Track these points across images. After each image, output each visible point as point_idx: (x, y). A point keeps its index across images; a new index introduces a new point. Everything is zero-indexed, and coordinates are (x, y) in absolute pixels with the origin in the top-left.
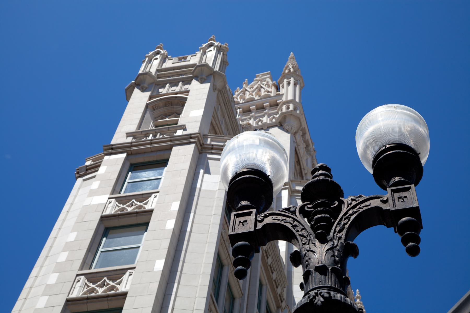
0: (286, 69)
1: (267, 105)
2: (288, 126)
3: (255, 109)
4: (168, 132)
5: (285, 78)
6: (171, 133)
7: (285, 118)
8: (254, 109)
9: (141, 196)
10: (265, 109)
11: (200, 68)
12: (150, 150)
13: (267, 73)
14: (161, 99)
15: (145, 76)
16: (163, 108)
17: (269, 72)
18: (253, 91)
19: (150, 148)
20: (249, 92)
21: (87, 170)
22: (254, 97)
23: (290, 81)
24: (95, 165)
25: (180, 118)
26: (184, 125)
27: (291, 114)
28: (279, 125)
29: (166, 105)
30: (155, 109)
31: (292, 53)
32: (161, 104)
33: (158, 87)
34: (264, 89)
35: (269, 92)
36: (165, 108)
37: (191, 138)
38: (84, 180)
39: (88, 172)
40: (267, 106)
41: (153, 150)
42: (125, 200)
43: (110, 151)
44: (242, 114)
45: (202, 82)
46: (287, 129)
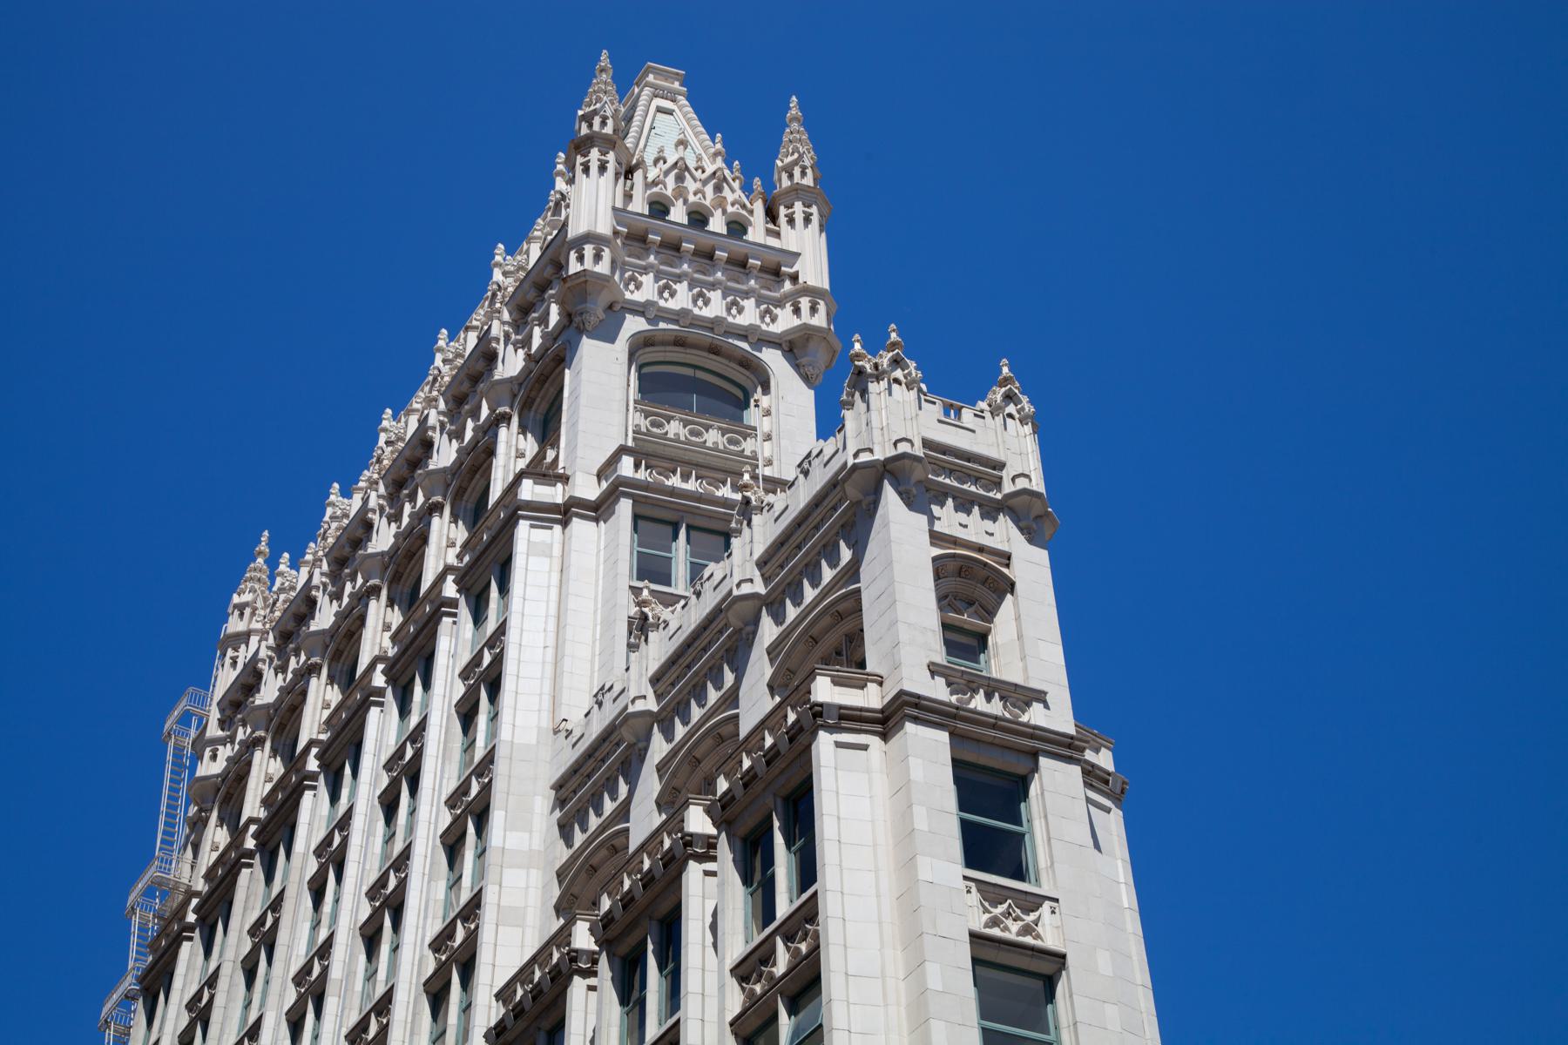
0: (797, 164)
1: (757, 265)
2: (813, 368)
3: (725, 259)
4: (1013, 695)
5: (798, 199)
6: (1018, 699)
7: (808, 340)
8: (721, 260)
9: (1023, 897)
10: (747, 271)
11: (1030, 498)
12: (991, 740)
13: (677, 74)
14: (954, 556)
15: (915, 464)
16: (954, 579)
17: (684, 72)
18: (705, 182)
19: (995, 737)
20: (695, 180)
21: (841, 718)
22: (707, 203)
23: (811, 214)
24: (859, 713)
25: (992, 625)
26: (1045, 693)
27: (825, 338)
28: (786, 349)
29: (960, 572)
30: (941, 575)
31: (794, 98)
32: (952, 566)
33: (928, 495)
34: (733, 191)
35: (744, 206)
36: (958, 579)
37: (1069, 746)
38: (839, 745)
39: (845, 724)
40: (754, 267)
41: (996, 741)
42: (994, 893)
43: (915, 712)
44: (690, 257)
45: (1031, 541)
46: (808, 373)
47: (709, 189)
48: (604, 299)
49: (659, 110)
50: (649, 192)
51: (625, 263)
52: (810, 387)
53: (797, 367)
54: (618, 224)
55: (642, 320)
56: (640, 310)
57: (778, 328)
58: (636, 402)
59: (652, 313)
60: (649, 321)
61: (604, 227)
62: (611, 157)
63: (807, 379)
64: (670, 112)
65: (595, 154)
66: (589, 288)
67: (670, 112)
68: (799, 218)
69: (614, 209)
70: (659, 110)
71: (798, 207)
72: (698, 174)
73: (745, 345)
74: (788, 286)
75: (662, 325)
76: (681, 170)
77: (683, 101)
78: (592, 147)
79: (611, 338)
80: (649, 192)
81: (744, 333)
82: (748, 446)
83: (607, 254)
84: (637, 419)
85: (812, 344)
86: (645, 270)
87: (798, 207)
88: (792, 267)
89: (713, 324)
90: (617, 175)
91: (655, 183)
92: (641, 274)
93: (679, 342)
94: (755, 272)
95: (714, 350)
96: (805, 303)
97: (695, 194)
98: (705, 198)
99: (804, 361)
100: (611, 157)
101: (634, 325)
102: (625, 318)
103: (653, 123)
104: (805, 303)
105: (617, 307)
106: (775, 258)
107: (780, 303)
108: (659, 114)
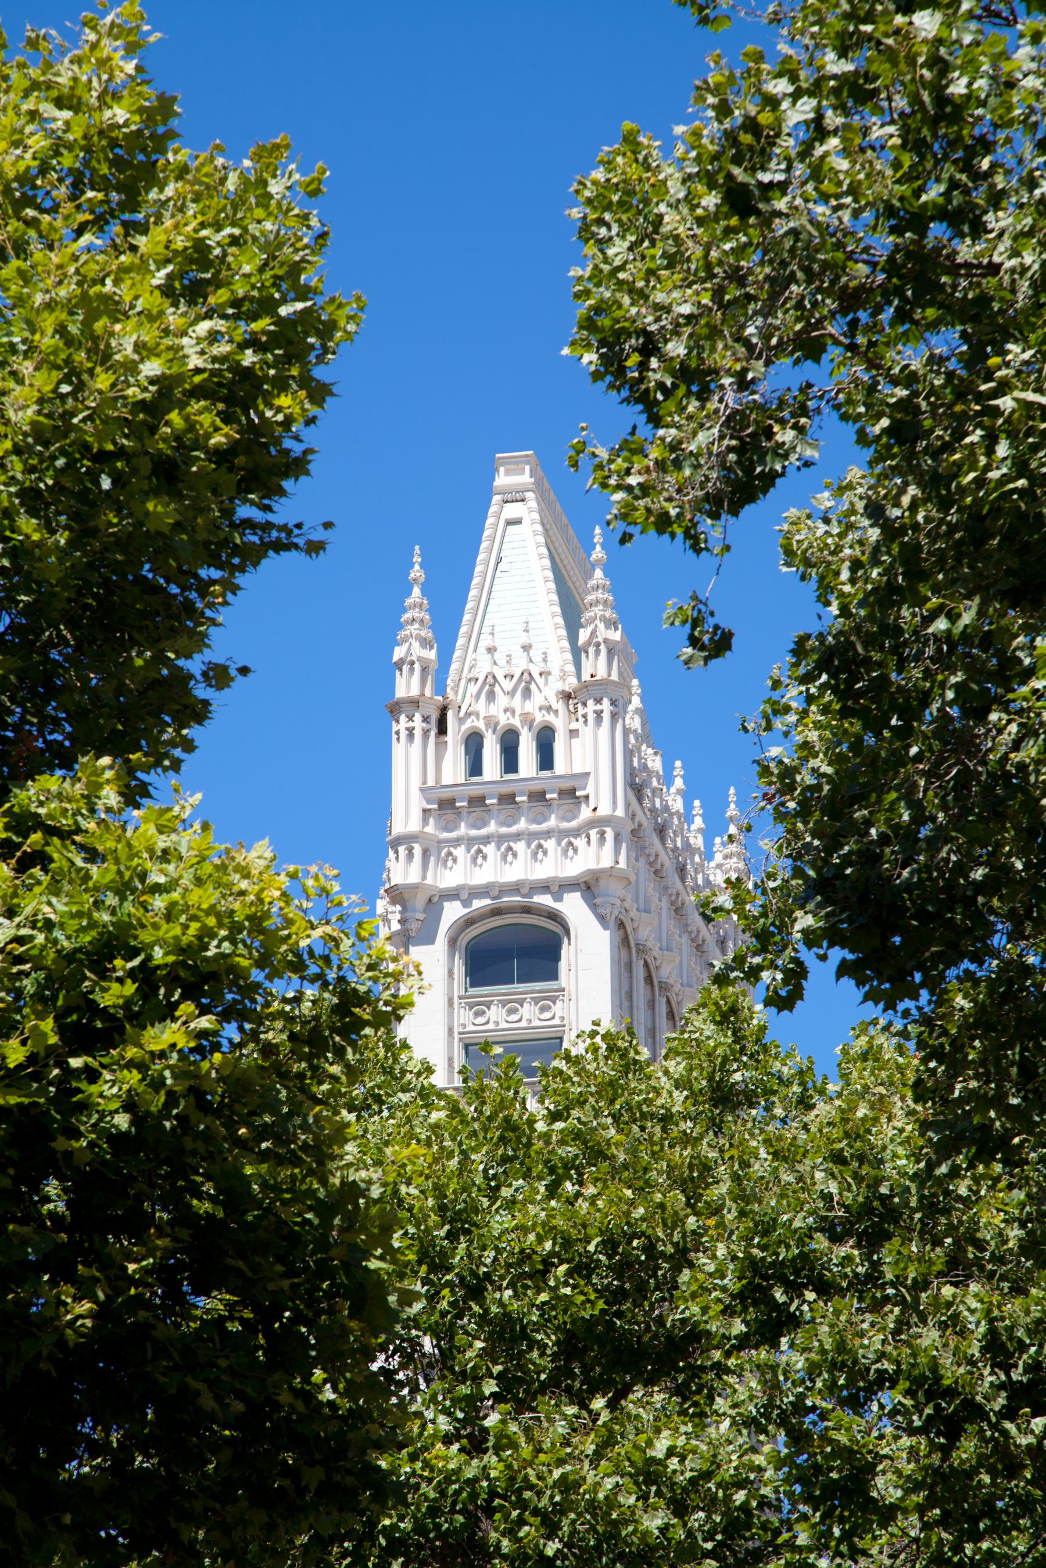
7: (597, 879)
18: (512, 694)
35: (549, 709)
47: (517, 701)
48: (420, 902)
49: (509, 523)
50: (464, 728)
51: (440, 842)
52: (605, 928)
53: (594, 907)
54: (429, 802)
55: (457, 904)
56: (453, 894)
57: (574, 868)
58: (460, 998)
59: (464, 895)
60: (466, 903)
61: (414, 825)
62: (418, 717)
63: (602, 919)
64: (518, 522)
65: (403, 718)
66: (406, 896)
67: (518, 522)
68: (591, 717)
69: (423, 790)
70: (509, 523)
71: (590, 702)
72: (508, 685)
73: (545, 900)
74: (585, 813)
75: (478, 904)
76: (490, 688)
77: (530, 495)
78: (400, 713)
79: (430, 940)
80: (464, 728)
81: (544, 887)
82: (558, 1008)
83: (417, 850)
84: (465, 1018)
85: (602, 883)
86: (457, 842)
87: (590, 702)
88: (584, 788)
89: (516, 888)
90: (426, 733)
91: (468, 714)
92: (455, 847)
93: (496, 912)
94: (555, 802)
95: (527, 910)
96: (593, 833)
97: (505, 711)
98: (513, 712)
99: (598, 901)
100: (418, 717)
101: (453, 912)
102: (442, 908)
103: (500, 550)
104: (593, 833)
105: (435, 899)
106: (566, 785)
107: (576, 833)
108: (511, 529)
